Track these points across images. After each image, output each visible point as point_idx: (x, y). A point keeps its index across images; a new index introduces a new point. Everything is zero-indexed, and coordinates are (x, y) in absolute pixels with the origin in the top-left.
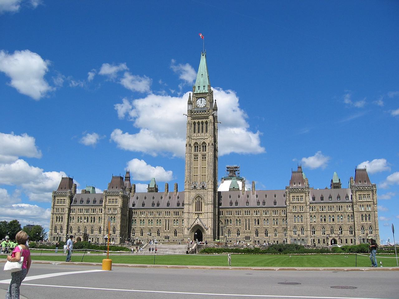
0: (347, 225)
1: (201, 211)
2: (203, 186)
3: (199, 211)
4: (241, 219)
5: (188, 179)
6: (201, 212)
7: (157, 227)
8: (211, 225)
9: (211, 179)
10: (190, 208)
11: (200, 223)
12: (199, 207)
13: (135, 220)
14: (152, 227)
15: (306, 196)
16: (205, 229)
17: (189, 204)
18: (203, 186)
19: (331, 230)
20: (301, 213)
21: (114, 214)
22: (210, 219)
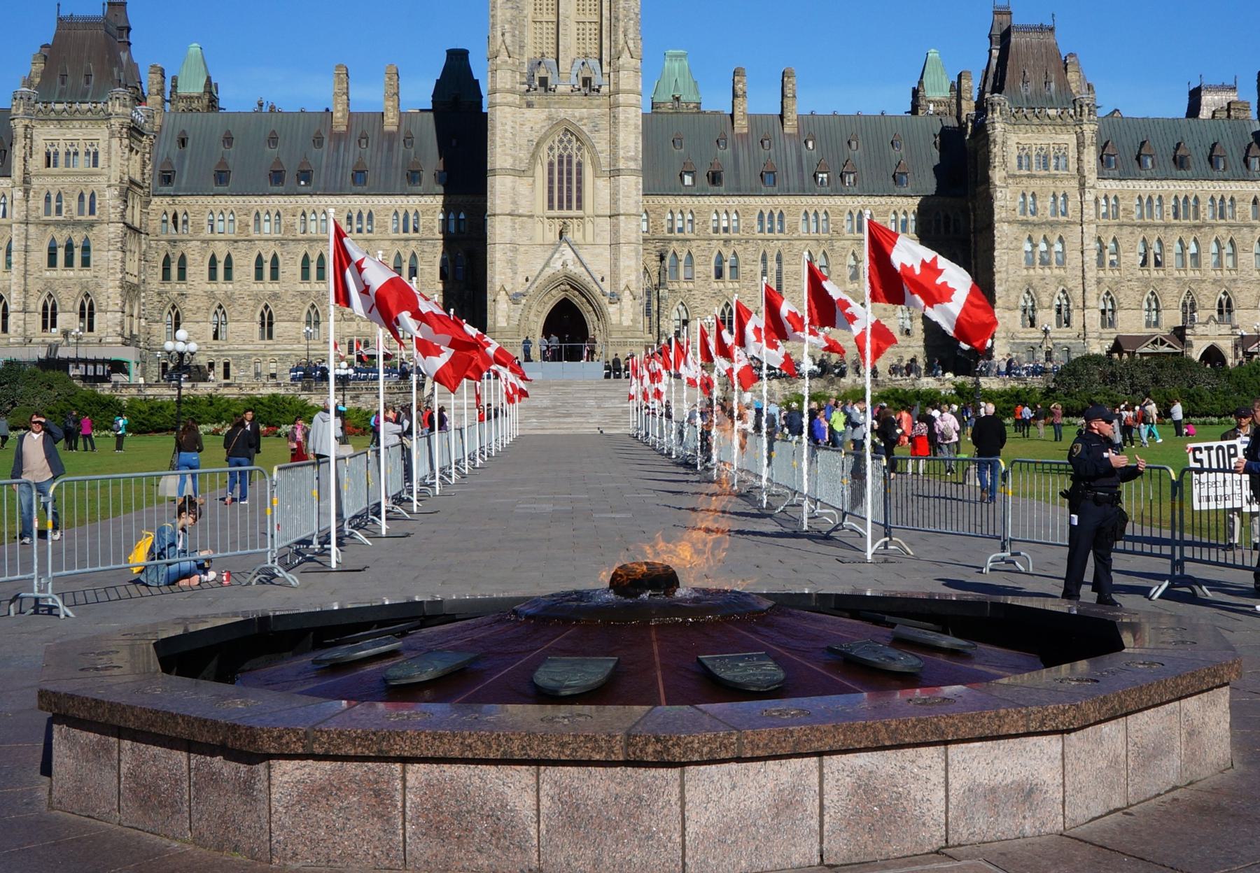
0: (1251, 282)
1: (579, 207)
2: (586, 81)
3: (569, 208)
4: (739, 249)
5: (508, 41)
6: (580, 213)
7: (302, 293)
8: (633, 277)
9: (631, 44)
10: (513, 193)
11: (575, 269)
12: (565, 188)
13: (183, 259)
14: (275, 296)
15: (1080, 145)
16: (606, 300)
17: (519, 173)
18: (586, 81)
19: (1184, 305)
20: (1058, 223)
21: (79, 223)
22: (632, 247)
